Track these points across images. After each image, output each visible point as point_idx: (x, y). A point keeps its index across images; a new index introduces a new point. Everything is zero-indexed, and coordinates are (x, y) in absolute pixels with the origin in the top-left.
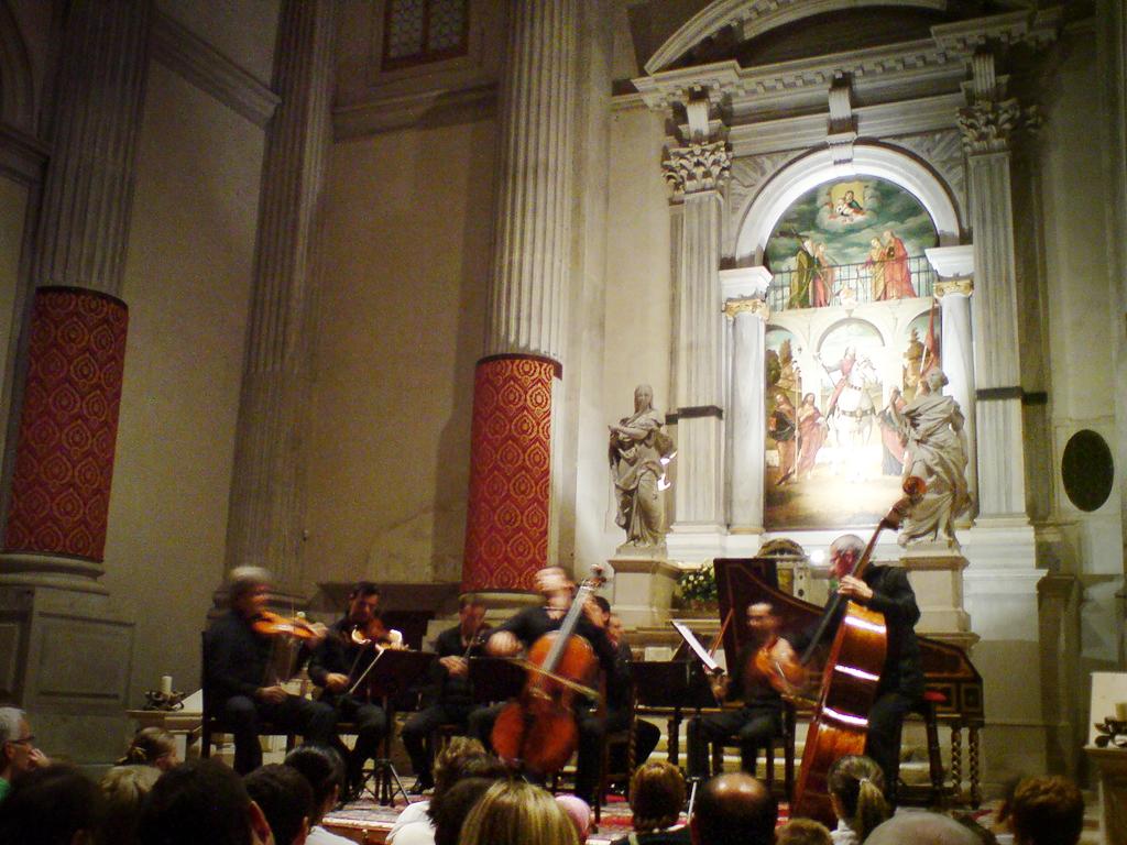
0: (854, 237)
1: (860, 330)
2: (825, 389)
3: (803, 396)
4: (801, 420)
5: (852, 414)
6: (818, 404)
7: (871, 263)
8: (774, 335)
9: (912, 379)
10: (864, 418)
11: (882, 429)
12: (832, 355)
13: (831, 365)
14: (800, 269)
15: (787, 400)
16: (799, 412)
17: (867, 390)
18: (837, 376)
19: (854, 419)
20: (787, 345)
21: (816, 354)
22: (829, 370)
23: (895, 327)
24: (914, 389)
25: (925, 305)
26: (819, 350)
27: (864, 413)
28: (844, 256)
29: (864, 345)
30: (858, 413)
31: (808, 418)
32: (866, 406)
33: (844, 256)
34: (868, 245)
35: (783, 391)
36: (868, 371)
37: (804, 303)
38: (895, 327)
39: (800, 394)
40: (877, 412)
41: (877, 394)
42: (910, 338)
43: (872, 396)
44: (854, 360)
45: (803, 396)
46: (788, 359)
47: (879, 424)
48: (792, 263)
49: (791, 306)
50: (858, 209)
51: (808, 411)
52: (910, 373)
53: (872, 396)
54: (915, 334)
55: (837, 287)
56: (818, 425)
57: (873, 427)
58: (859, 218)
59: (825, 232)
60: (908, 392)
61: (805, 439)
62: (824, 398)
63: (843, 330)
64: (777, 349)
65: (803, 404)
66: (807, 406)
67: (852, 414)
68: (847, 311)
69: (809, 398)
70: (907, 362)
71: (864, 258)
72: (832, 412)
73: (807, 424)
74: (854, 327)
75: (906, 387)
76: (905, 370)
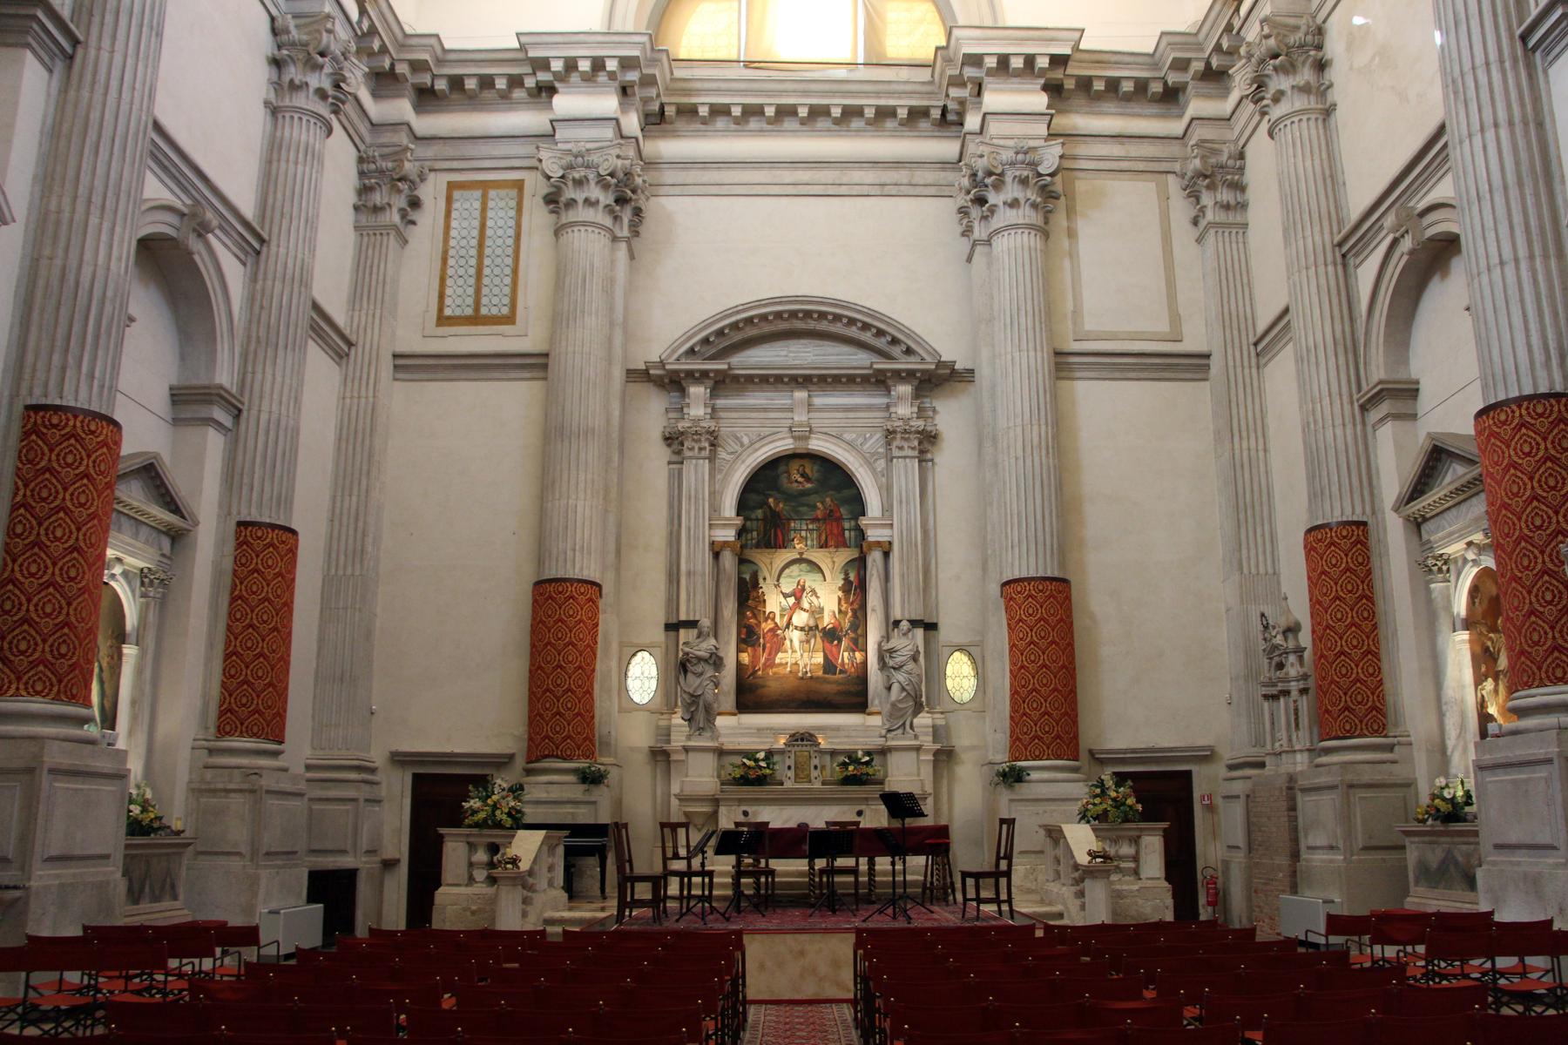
0: (804, 499)
2: (783, 610)
5: (802, 629)
6: (778, 620)
7: (815, 520)
8: (744, 568)
12: (788, 585)
14: (765, 519)
15: (755, 616)
18: (792, 600)
20: (755, 576)
22: (786, 596)
25: (854, 554)
27: (811, 629)
28: (797, 512)
29: (811, 580)
32: (812, 623)
33: (797, 512)
34: (814, 507)
35: (753, 610)
37: (768, 545)
44: (803, 589)
46: (756, 585)
48: (759, 513)
49: (758, 546)
50: (808, 479)
51: (770, 625)
54: (847, 574)
55: (792, 534)
58: (808, 486)
59: (784, 493)
62: (782, 616)
63: (795, 568)
64: (747, 577)
65: (766, 619)
67: (802, 629)
70: (840, 594)
71: (812, 515)
72: (788, 627)
74: (804, 566)
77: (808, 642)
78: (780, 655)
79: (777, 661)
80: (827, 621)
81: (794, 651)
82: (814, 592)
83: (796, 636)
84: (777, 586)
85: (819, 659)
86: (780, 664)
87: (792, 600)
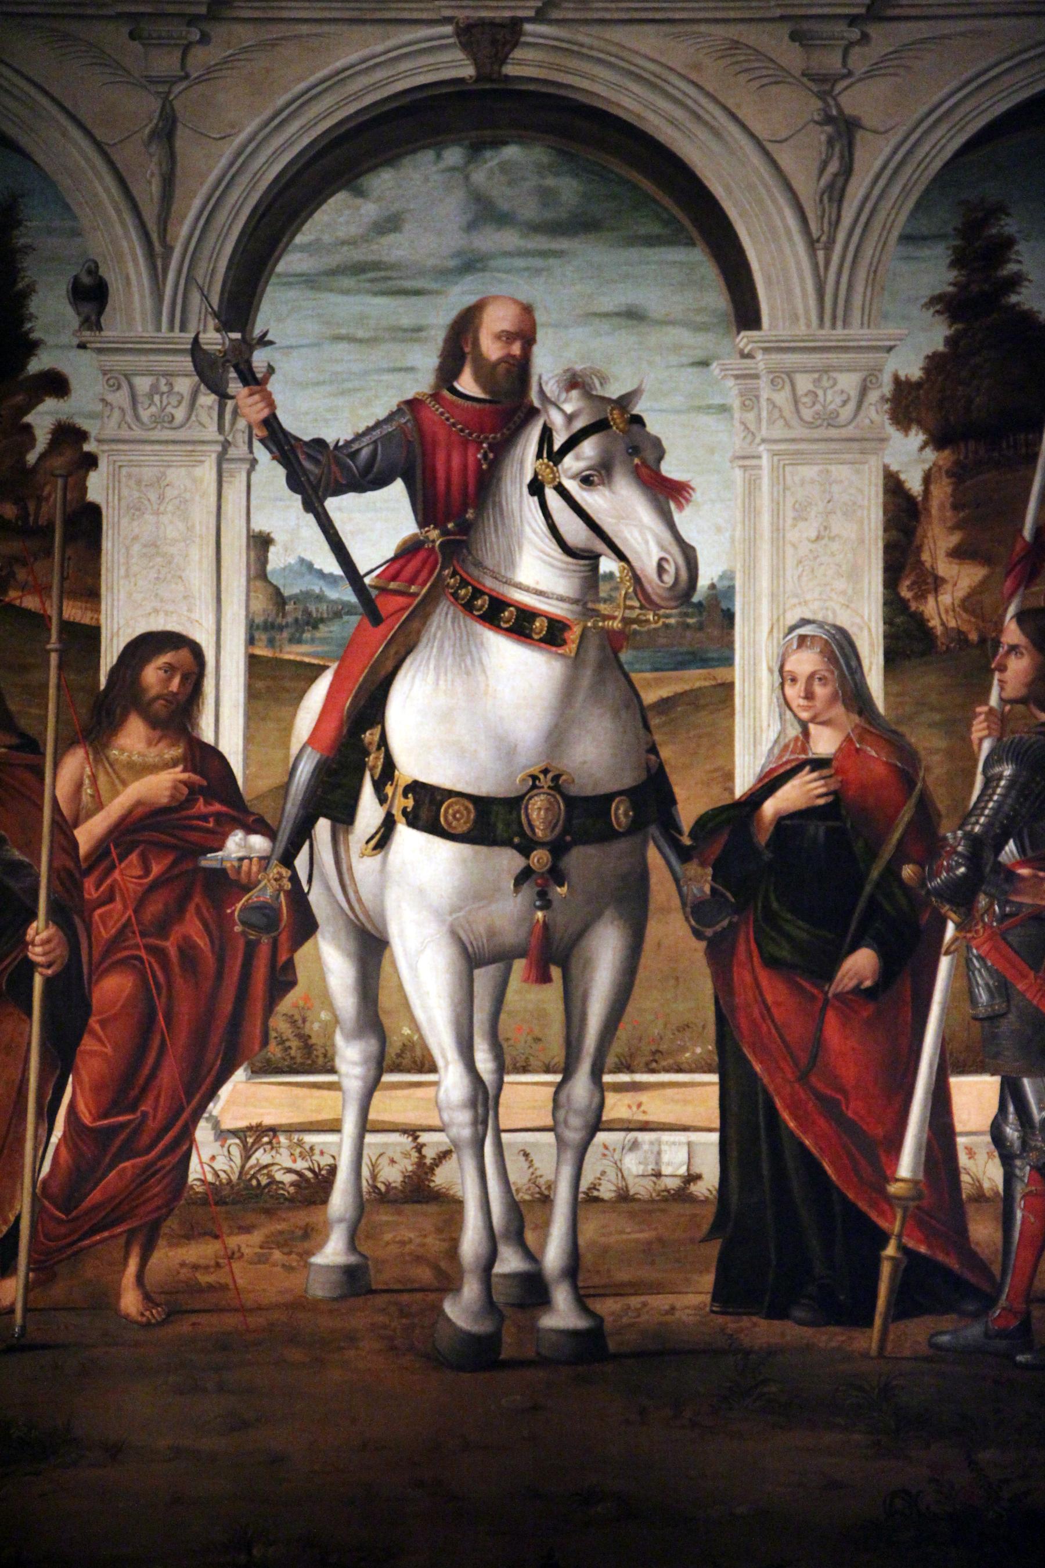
1: (569, 188)
3: (109, 655)
4: (87, 834)
6: (225, 722)
9: (955, 585)
10: (581, 859)
11: (720, 955)
13: (336, 432)
16: (68, 774)
17: (613, 643)
18: (380, 523)
19: (507, 861)
21: (213, 339)
22: (318, 473)
23: (835, 193)
24: (976, 658)
26: (239, 306)
27: (585, 817)
30: (538, 812)
31: (138, 829)
32: (596, 757)
36: (624, 510)
38: (835, 193)
39: (87, 638)
40: (689, 811)
41: (694, 678)
42: (935, 273)
43: (649, 697)
44: (511, 403)
45: (109, 655)
47: (699, 913)
52: (938, 543)
53: (649, 697)
56: (224, 884)
57: (654, 930)
60: (928, 680)
61: (113, 989)
62: (273, 683)
63: (422, 198)
66: (133, 738)
68: (470, 35)
69: (152, 675)
70: (910, 455)
72: (332, 797)
73: (129, 873)
74: (516, 167)
75: (908, 638)
76: (903, 513)
77: (553, 954)
78: (243, 1099)
79: (210, 1159)
80: (762, 732)
81: (399, 1057)
82: (625, 441)
83: (421, 890)
84: (231, 368)
85: (674, 1136)
86: (246, 1199)
87: (380, 523)
